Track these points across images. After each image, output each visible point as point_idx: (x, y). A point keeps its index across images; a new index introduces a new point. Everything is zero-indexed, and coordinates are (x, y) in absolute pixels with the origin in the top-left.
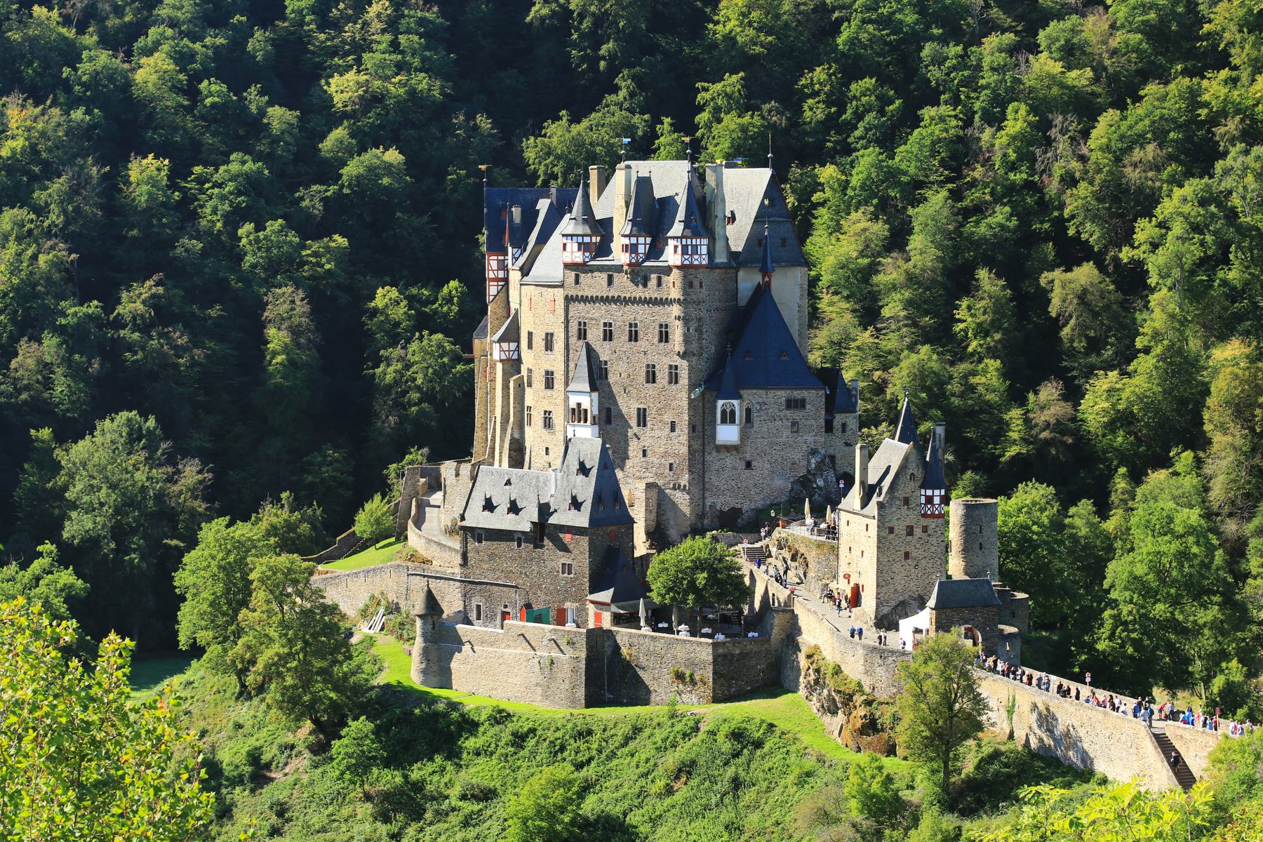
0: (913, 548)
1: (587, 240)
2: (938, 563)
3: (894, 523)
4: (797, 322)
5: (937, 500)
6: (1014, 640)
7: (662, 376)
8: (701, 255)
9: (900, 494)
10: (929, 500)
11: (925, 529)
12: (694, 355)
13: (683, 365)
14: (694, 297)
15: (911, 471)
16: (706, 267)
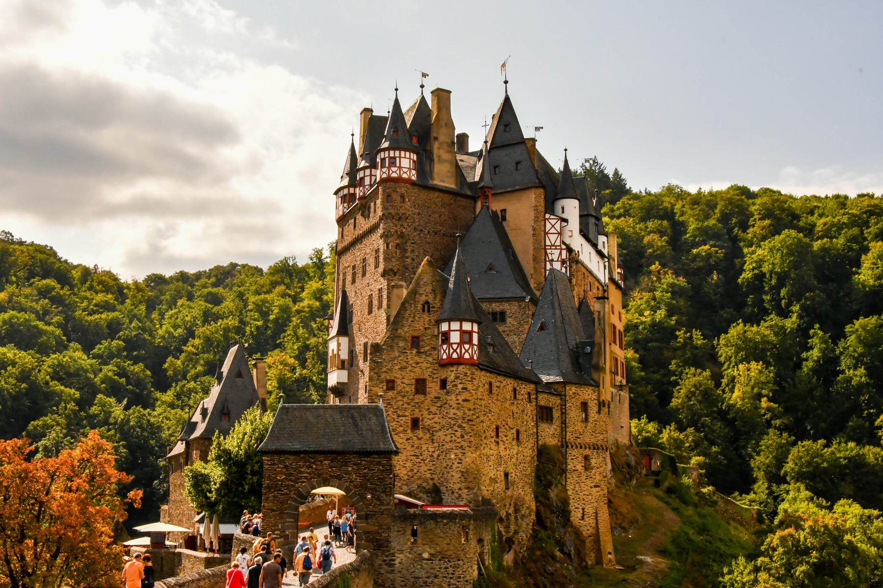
0: (425, 413)
1: (346, 191)
2: (458, 434)
3: (396, 374)
4: (532, 248)
5: (455, 337)
6: (431, 524)
7: (375, 303)
8: (400, 167)
9: (406, 331)
10: (446, 337)
11: (443, 383)
12: (395, 274)
13: (383, 283)
14: (392, 211)
15: (423, 298)
16: (413, 183)
